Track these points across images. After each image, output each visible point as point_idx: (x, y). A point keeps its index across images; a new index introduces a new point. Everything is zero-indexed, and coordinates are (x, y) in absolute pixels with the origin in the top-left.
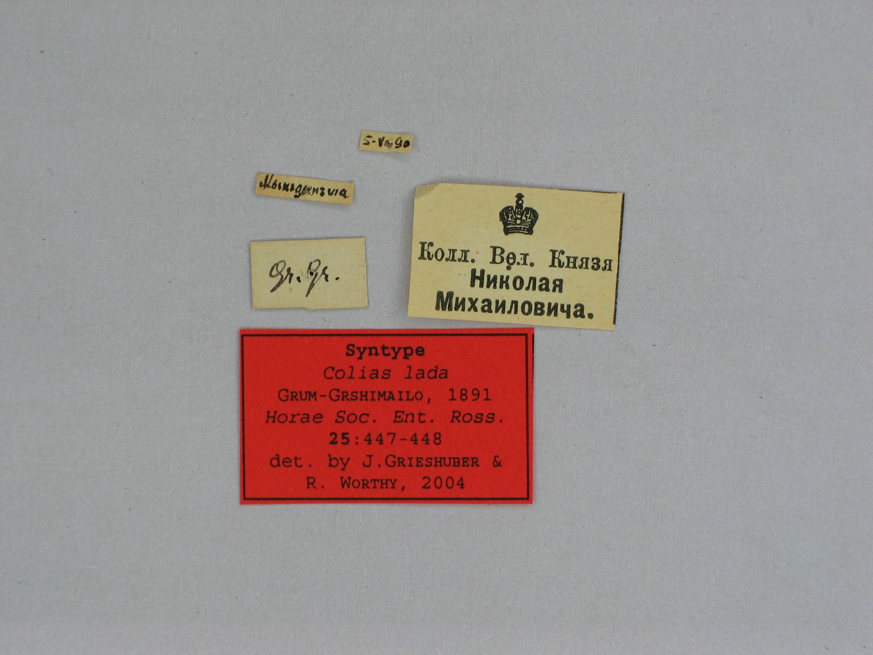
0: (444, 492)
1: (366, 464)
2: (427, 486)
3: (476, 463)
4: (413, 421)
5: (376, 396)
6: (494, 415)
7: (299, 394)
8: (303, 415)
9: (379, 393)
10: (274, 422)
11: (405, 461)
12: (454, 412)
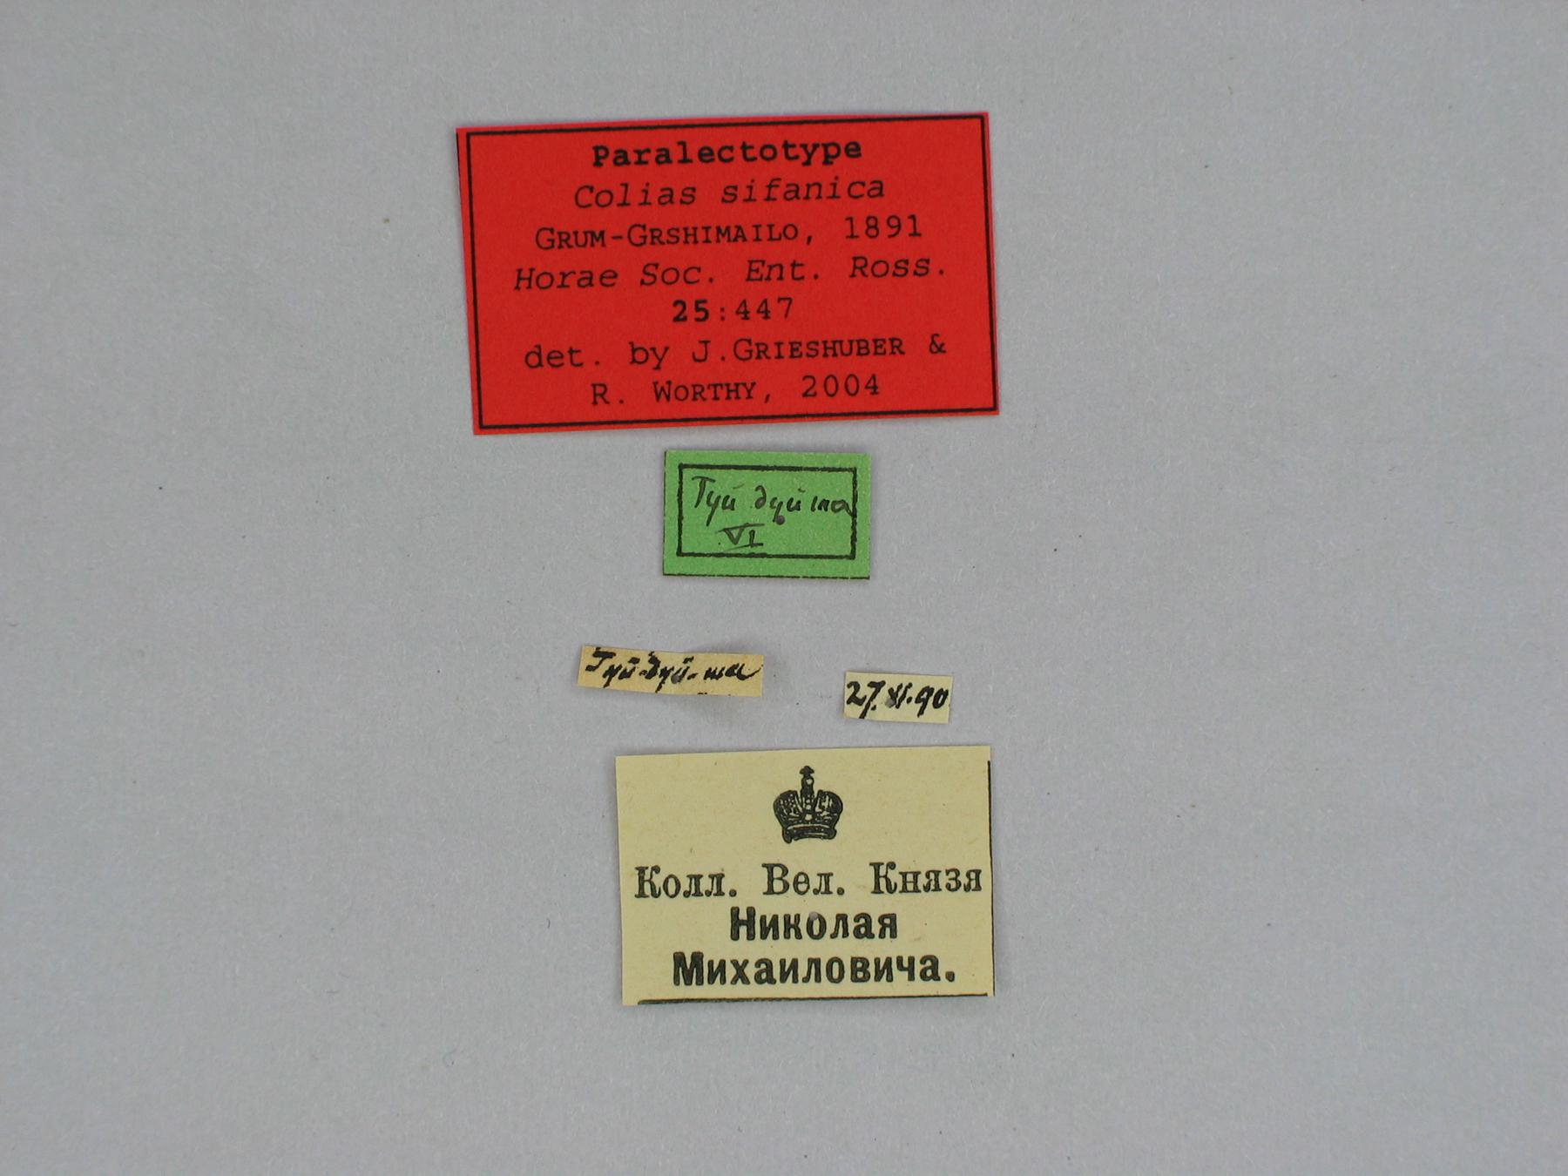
0: (842, 401)
1: (697, 357)
2: (811, 393)
3: (898, 348)
4: (780, 278)
5: (712, 234)
6: (928, 261)
7: (573, 237)
8: (582, 273)
9: (718, 229)
10: (529, 287)
11: (770, 349)
12: (855, 259)
